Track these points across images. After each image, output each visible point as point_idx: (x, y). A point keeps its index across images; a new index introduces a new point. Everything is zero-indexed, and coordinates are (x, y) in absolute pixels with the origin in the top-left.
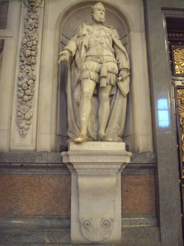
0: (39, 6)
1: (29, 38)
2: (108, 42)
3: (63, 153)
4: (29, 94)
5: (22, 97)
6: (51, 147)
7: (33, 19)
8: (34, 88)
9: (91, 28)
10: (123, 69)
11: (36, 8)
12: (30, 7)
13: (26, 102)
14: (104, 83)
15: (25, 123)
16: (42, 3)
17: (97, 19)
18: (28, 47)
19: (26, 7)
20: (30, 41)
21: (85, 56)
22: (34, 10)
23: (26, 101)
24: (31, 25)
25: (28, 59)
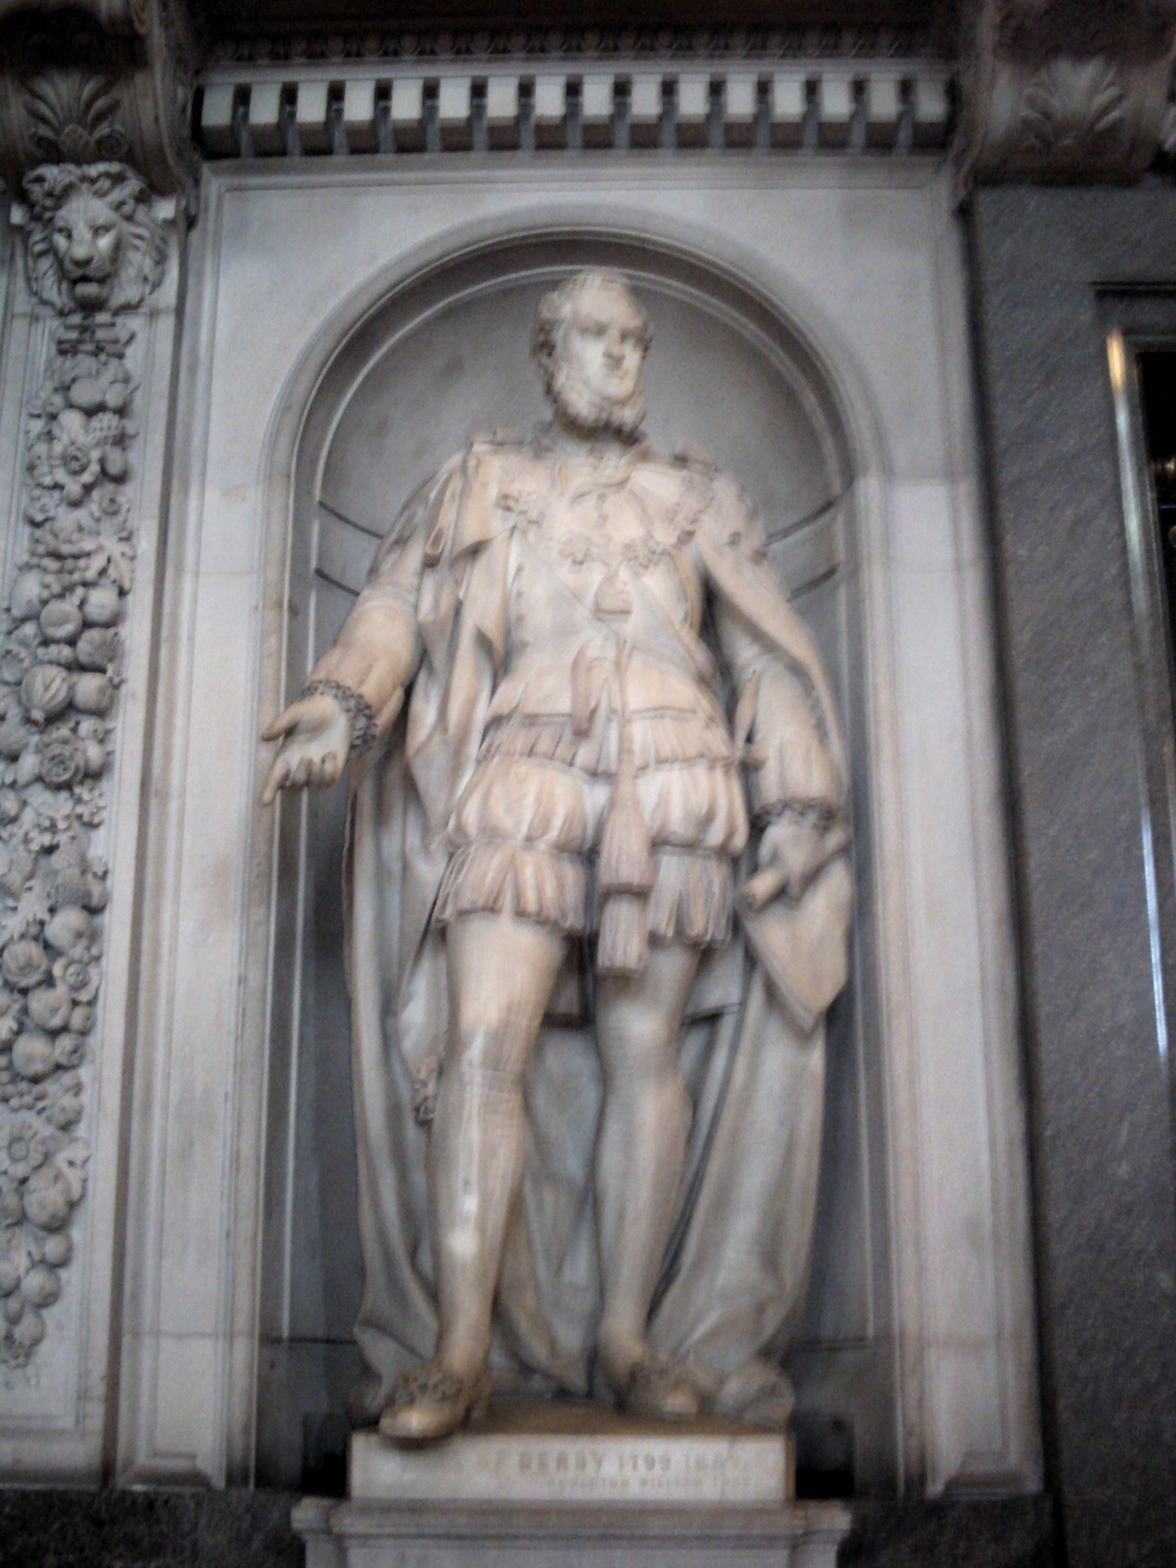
0: (141, 300)
1: (52, 564)
2: (660, 598)
3: (306, 1513)
4: (56, 1022)
6: (229, 1440)
7: (92, 412)
8: (93, 971)
9: (529, 481)
10: (786, 805)
11: (119, 320)
12: (71, 312)
13: (37, 1089)
14: (622, 940)
15: (29, 1254)
16: (162, 275)
17: (582, 403)
18: (46, 642)
19: (46, 312)
20: (61, 596)
21: (482, 714)
22: (101, 334)
23: (36, 1080)
24: (73, 462)
25: (46, 738)
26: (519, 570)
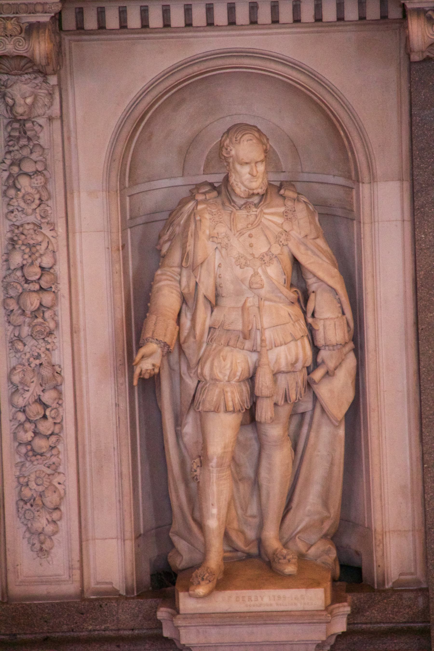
5: (29, 443)
10: (326, 345)
15: (47, 519)
26: (219, 266)
